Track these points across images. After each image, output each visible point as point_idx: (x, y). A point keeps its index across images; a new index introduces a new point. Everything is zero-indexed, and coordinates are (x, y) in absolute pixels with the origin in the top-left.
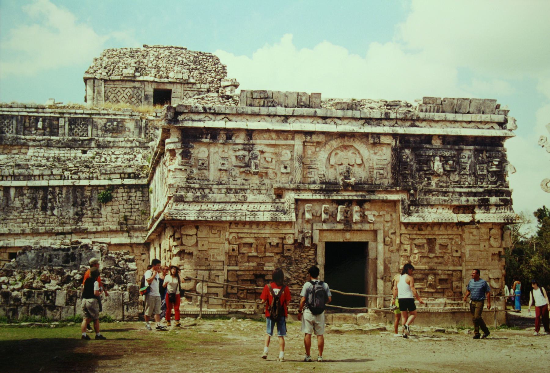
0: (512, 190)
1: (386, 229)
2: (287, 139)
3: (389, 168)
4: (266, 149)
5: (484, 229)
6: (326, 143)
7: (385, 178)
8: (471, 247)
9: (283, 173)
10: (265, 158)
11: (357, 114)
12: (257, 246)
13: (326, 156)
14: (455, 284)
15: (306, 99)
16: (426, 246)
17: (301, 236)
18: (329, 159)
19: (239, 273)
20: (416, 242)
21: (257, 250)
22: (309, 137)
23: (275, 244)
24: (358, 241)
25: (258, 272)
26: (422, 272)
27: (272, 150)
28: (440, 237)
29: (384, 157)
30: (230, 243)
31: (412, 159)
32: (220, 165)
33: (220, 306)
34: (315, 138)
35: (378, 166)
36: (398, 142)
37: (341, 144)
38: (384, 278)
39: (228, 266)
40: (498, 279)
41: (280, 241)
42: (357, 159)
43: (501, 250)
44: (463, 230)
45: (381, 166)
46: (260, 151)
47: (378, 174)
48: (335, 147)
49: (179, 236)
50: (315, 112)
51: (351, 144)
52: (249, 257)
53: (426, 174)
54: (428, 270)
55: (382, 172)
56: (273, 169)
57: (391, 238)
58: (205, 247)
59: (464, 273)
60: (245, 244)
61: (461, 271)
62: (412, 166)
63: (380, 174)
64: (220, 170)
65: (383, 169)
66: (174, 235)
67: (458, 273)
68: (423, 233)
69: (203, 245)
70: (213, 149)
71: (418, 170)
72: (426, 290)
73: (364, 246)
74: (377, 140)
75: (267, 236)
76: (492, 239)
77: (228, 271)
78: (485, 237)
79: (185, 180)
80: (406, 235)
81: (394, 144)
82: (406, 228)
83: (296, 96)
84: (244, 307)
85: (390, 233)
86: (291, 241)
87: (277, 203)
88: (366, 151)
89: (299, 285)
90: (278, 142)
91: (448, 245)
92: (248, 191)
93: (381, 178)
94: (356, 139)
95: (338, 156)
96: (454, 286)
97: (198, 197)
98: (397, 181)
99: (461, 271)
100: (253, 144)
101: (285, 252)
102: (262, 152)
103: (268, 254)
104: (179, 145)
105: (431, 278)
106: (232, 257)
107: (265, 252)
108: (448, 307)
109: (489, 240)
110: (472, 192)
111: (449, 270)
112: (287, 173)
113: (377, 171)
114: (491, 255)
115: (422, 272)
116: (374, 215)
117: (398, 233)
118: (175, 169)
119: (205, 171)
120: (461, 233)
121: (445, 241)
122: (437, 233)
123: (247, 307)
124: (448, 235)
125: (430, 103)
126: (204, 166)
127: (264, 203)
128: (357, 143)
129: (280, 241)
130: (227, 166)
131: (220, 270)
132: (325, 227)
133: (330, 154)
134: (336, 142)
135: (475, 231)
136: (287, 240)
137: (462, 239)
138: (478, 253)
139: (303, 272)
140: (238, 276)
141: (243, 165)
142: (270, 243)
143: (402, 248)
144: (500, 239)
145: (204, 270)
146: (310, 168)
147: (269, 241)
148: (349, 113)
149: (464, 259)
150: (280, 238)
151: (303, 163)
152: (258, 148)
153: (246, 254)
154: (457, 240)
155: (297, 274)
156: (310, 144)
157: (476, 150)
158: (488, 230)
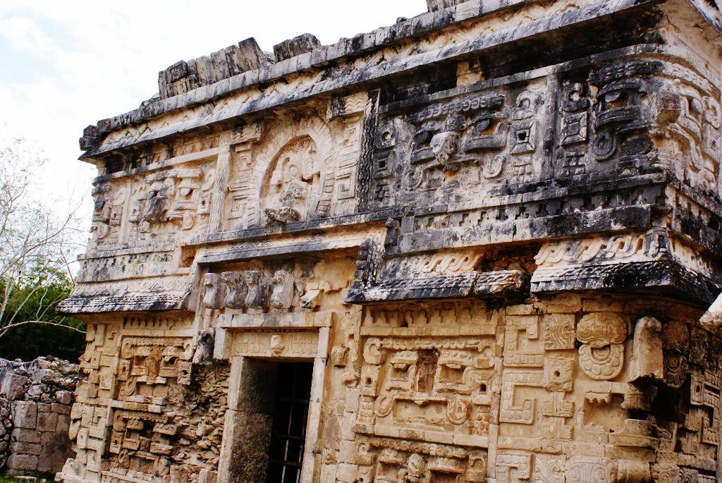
5: (557, 318)
8: (520, 376)
11: (304, 60)
15: (239, 59)
16: (412, 370)
19: (126, 415)
20: (398, 359)
22: (239, 134)
23: (167, 359)
24: (295, 355)
25: (145, 416)
26: (395, 444)
28: (447, 344)
30: (120, 356)
31: (408, 138)
34: (251, 133)
36: (377, 104)
37: (291, 138)
38: (325, 452)
39: (115, 398)
43: (623, 388)
45: (347, 171)
48: (282, 144)
50: (244, 78)
52: (139, 385)
55: (347, 183)
58: (95, 364)
60: (140, 359)
61: (486, 450)
62: (402, 155)
67: (481, 456)
68: (405, 332)
71: (415, 163)
75: (161, 342)
76: (584, 351)
77: (114, 409)
81: (370, 109)
82: (374, 321)
83: (223, 57)
85: (347, 336)
86: (187, 354)
87: (181, 275)
91: (463, 368)
92: (153, 256)
97: (98, 272)
98: (366, 201)
99: (486, 450)
100: (170, 167)
102: (178, 180)
103: (160, 380)
105: (414, 460)
110: (531, 203)
111: (453, 445)
114: (580, 405)
117: (357, 337)
120: (493, 332)
121: (458, 359)
122: (434, 334)
127: (163, 276)
130: (137, 213)
132: (240, 321)
133: (276, 159)
134: (286, 133)
135: (531, 324)
136: (184, 353)
137: (501, 352)
138: (542, 396)
140: (126, 421)
142: (164, 357)
143: (364, 377)
144: (617, 351)
148: (293, 64)
149: (494, 413)
152: (171, 173)
155: (209, 427)
157: (562, 77)
158: (571, 319)
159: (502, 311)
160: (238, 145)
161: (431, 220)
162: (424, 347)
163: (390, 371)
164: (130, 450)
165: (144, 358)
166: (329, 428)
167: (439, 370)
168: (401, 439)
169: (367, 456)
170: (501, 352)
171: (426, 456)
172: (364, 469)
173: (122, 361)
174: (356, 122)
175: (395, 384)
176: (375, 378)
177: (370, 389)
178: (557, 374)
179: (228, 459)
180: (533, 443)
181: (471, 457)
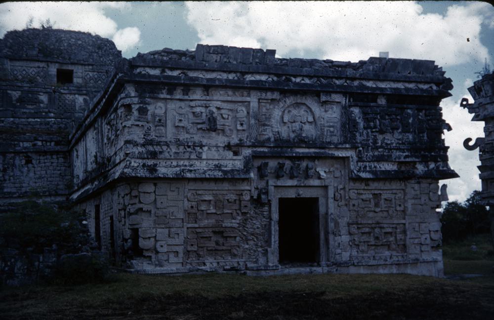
0: (448, 147)
1: (336, 185)
2: (243, 96)
3: (338, 125)
4: (224, 105)
6: (279, 100)
7: (335, 136)
8: (413, 201)
9: (238, 130)
10: (222, 115)
12: (215, 202)
13: (280, 114)
14: (399, 236)
16: (372, 200)
17: (256, 192)
18: (282, 118)
19: (199, 230)
20: (364, 197)
21: (215, 207)
22: (264, 94)
23: (233, 201)
25: (217, 230)
26: (369, 226)
27: (229, 106)
28: (385, 192)
29: (334, 115)
30: (188, 200)
32: (177, 121)
33: (181, 265)
34: (269, 95)
35: (329, 124)
40: (437, 231)
41: (237, 198)
42: (309, 117)
44: (405, 185)
45: (331, 124)
46: (217, 108)
47: (329, 131)
49: (137, 194)
51: (303, 102)
52: (208, 213)
53: (372, 132)
54: (376, 224)
55: (332, 129)
56: (228, 126)
57: (340, 194)
59: (407, 225)
60: (202, 201)
61: (404, 224)
63: (331, 132)
64: (178, 127)
65: (333, 127)
66: (130, 193)
67: (401, 225)
69: (162, 203)
70: (171, 106)
71: (365, 128)
72: (373, 243)
73: (315, 200)
74: (329, 99)
75: (225, 192)
77: (188, 228)
78: (426, 191)
79: (143, 136)
80: (354, 191)
81: (344, 103)
84: (204, 264)
86: (247, 198)
88: (318, 109)
89: (254, 241)
90: (234, 99)
93: (331, 136)
94: (308, 97)
95: (291, 113)
96: (398, 238)
98: (347, 139)
99: (404, 224)
101: (242, 208)
102: (219, 109)
103: (226, 211)
104: (136, 100)
105: (377, 230)
106: (192, 215)
107: (223, 208)
108: (395, 259)
109: (429, 194)
111: (393, 224)
112: (244, 130)
113: (328, 128)
115: (369, 226)
116: (325, 172)
118: (132, 125)
119: (162, 128)
120: (404, 188)
121: (390, 196)
122: (382, 188)
123: (208, 264)
124: (392, 189)
125: (376, 63)
126: (161, 122)
128: (308, 101)
129: (237, 198)
131: (180, 227)
133: (284, 112)
135: (416, 186)
136: (244, 197)
137: (405, 194)
139: (258, 228)
140: (197, 233)
141: (201, 121)
142: (228, 200)
143: (351, 204)
145: (163, 228)
146: (264, 125)
147: (226, 198)
149: (407, 213)
150: (237, 195)
151: (258, 121)
153: (205, 211)
154: (400, 195)
156: (265, 101)
158: (428, 185)
159: (406, 182)
160: (263, 99)
161: (378, 150)
162: (376, 193)
163: (360, 201)
164: (207, 247)
165: (210, 201)
166: (337, 224)
167: (382, 201)
168: (373, 224)
169: (355, 231)
170: (405, 194)
171: (381, 228)
172: (356, 236)
173: (190, 203)
174: (334, 105)
175: (367, 206)
176: (356, 204)
177: (355, 208)
178: (425, 200)
179: (277, 242)
180: (418, 220)
181: (398, 227)
